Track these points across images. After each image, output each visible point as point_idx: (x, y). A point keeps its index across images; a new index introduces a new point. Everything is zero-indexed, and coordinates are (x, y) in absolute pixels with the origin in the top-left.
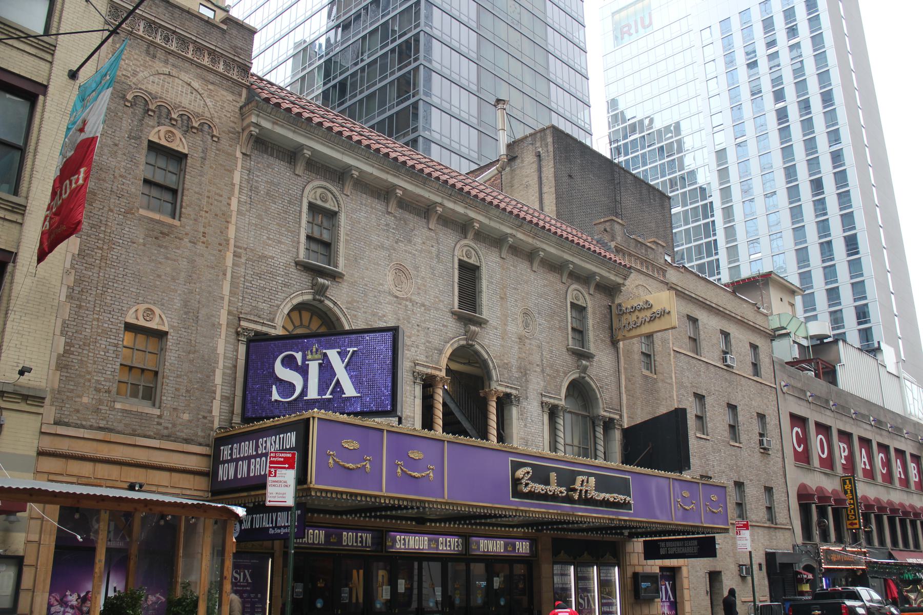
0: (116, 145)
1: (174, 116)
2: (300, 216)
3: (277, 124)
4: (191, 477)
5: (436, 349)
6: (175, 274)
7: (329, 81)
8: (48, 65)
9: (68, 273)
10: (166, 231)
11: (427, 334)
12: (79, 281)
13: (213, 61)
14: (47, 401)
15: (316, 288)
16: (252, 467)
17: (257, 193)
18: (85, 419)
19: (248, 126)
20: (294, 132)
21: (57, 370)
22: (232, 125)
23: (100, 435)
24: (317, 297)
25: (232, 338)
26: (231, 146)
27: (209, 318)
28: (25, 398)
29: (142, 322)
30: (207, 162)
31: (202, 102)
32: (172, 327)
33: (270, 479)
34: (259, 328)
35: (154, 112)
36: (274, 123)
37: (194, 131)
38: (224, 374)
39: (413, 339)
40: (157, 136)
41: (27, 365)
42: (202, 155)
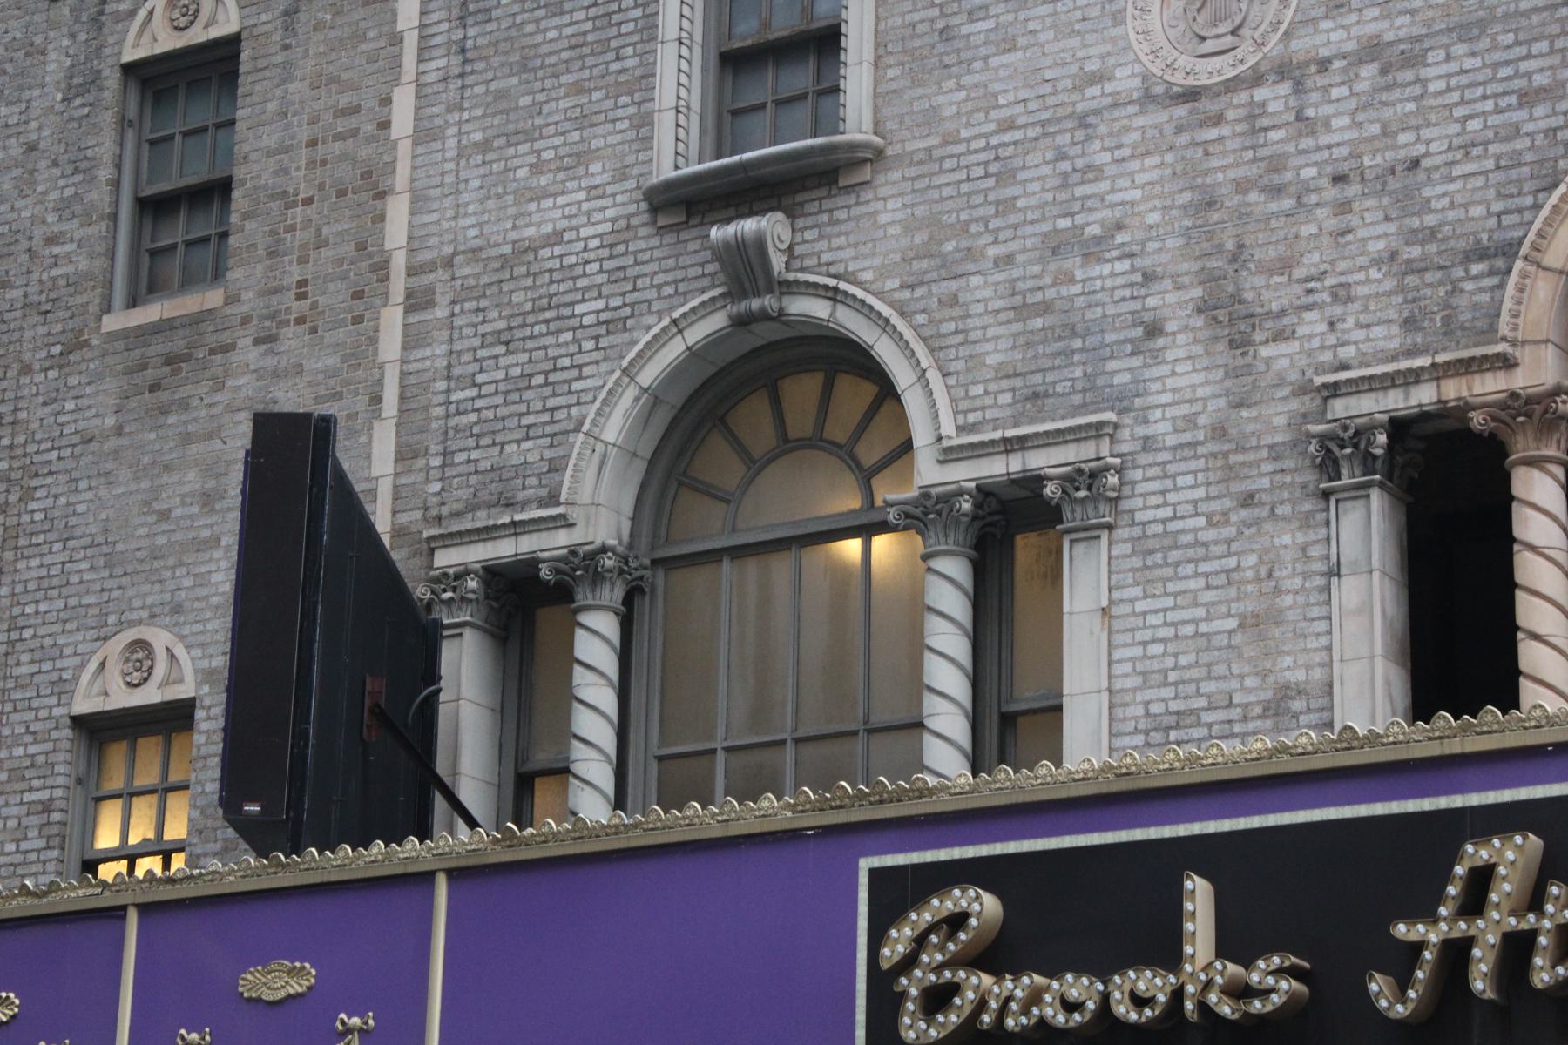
0: (32, 148)
5: (1482, 254)
6: (212, 483)
10: (179, 345)
11: (1408, 202)
24: (735, 309)
29: (123, 698)
30: (302, 16)
39: (1313, 260)
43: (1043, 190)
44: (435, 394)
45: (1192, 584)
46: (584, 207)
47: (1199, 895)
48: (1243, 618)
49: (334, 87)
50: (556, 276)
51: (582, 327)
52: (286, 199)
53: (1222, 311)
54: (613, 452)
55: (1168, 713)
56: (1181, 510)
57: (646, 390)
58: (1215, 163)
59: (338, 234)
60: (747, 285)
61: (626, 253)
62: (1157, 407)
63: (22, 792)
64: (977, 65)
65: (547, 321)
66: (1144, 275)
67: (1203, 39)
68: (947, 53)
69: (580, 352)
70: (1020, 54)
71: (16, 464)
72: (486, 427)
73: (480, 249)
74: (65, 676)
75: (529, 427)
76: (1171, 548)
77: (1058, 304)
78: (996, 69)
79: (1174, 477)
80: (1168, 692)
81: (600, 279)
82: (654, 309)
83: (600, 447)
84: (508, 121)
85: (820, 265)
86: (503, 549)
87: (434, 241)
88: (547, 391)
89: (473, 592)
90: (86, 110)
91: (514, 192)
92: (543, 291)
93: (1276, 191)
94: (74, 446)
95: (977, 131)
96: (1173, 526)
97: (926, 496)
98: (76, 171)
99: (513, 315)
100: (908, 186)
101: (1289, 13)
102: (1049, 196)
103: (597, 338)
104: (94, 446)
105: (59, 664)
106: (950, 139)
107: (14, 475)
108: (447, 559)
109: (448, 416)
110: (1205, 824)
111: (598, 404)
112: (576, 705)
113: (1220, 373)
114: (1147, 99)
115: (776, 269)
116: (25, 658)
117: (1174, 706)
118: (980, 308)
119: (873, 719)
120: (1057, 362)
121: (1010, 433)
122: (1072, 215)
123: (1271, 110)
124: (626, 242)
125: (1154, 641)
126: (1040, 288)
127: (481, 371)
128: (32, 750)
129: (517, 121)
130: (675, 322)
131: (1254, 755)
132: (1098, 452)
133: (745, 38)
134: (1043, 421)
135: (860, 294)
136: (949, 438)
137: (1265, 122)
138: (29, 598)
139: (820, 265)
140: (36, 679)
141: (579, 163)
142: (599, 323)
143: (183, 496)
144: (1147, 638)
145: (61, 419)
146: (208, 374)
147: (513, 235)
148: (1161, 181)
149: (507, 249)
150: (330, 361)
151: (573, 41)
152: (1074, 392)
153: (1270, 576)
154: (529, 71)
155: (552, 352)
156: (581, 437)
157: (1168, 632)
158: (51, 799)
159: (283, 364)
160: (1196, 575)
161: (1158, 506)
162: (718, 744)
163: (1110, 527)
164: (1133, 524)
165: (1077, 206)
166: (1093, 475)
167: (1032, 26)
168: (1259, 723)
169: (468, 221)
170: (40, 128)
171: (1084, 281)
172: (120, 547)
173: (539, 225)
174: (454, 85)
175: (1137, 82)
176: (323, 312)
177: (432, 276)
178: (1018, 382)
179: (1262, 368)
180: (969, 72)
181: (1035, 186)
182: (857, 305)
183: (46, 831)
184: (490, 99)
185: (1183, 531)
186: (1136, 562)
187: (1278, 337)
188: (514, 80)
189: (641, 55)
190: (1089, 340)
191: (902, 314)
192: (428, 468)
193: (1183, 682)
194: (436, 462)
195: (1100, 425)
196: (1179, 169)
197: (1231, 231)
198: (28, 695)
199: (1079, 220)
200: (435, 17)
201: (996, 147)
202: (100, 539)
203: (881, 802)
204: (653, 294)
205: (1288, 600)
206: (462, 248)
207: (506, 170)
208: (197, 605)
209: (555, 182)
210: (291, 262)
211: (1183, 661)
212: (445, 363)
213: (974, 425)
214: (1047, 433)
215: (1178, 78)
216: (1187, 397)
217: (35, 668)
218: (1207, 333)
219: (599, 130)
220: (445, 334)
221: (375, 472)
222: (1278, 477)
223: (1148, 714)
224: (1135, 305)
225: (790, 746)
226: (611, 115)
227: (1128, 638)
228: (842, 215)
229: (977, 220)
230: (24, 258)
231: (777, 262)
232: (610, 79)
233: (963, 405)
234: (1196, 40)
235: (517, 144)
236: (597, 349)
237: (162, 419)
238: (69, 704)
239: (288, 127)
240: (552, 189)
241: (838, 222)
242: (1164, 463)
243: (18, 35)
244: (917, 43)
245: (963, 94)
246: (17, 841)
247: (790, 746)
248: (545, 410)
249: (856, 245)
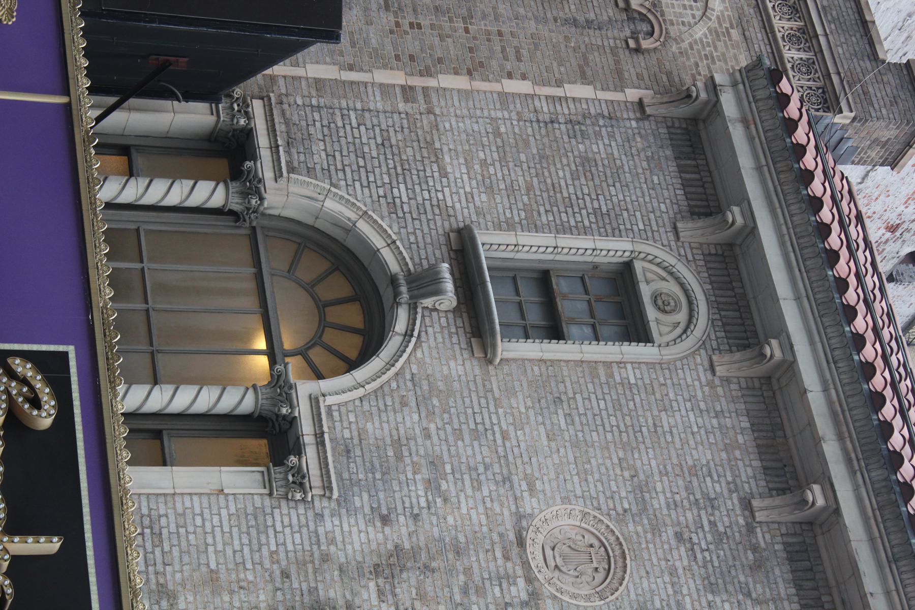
3: (747, 127)
20: (759, 168)
24: (401, 277)
26: (639, 77)
30: (573, 29)
36: (744, 121)
42: (581, 19)
43: (467, 457)
44: (354, 102)
45: (236, 543)
46: (462, 190)
47: (49, 545)
48: (217, 572)
49: (532, 47)
50: (421, 173)
51: (392, 188)
52: (468, 18)
53: (396, 560)
54: (318, 205)
55: (161, 528)
56: (280, 536)
57: (354, 224)
58: (481, 556)
59: (448, 47)
60: (414, 285)
61: (434, 214)
62: (341, 522)
64: (540, 419)
65: (395, 168)
66: (417, 515)
67: (553, 549)
68: (547, 401)
69: (377, 187)
70: (546, 443)
72: (334, 131)
73: (438, 130)
75: (334, 156)
76: (258, 530)
77: (401, 465)
78: (537, 430)
79: (300, 532)
80: (173, 528)
81: (420, 199)
82: (402, 230)
83: (321, 197)
84: (511, 147)
85: (426, 326)
86: (262, 140)
87: (443, 103)
88: (355, 167)
89: (238, 122)
91: (470, 150)
92: (413, 166)
93: (465, 592)
95: (502, 418)
96: (271, 532)
97: (291, 387)
99: (399, 148)
100: (471, 378)
101: (566, 598)
102: (464, 460)
103: (385, 197)
106: (497, 403)
108: (257, 107)
109: (341, 109)
110: (92, 549)
111: (347, 196)
112: (170, 181)
113: (360, 559)
114: (519, 517)
115: (423, 301)
117: (165, 531)
118: (400, 419)
119: (160, 355)
120: (368, 464)
121: (326, 436)
122: (453, 473)
123: (512, 588)
124: (441, 214)
125: (203, 520)
126: (411, 454)
127: (367, 129)
129: (511, 152)
130: (394, 242)
131: (132, 578)
132: (315, 487)
133: (557, 285)
134: (333, 455)
135: (409, 350)
136: (324, 401)
137: (505, 585)
139: (426, 326)
141: (486, 188)
142: (394, 198)
144: (205, 515)
147: (445, 149)
148: (472, 525)
149: (437, 145)
150: (373, 41)
151: (557, 185)
152: (350, 474)
153: (241, 588)
154: (540, 160)
155: (377, 170)
156: (327, 186)
157: (208, 528)
159: (373, 14)
160: (242, 545)
161: (282, 522)
162: (146, 264)
163: (270, 494)
164: (273, 508)
165: (458, 476)
166: (301, 485)
167: (562, 450)
168: (154, 581)
169: (454, 123)
171: (414, 480)
173: (451, 164)
174: (532, 116)
175: (529, 511)
176: (402, 38)
177: (423, 102)
178: (356, 441)
179: (362, 584)
180: (536, 414)
181: (470, 452)
182: (402, 348)
184: (524, 136)
185: (268, 537)
186: (250, 510)
187: (380, 593)
188: (535, 151)
189: (548, 225)
190: (380, 483)
191: (397, 374)
192: (311, 97)
193: (179, 537)
194: (314, 102)
195: (331, 489)
196: (479, 535)
197: (442, 565)
199: (450, 477)
200: (572, 106)
201: (492, 429)
203: (107, 359)
204: (410, 230)
205: (227, 598)
206: (438, 119)
207: (483, 146)
209: (476, 173)
210: (431, 20)
211: (191, 537)
212: (372, 108)
213: (332, 416)
214: (326, 458)
215: (531, 535)
216: (346, 540)
218: (383, 551)
219: (506, 200)
220: (389, 108)
221: (308, 66)
222: (298, 592)
223: (160, 516)
224: (400, 509)
225: (144, 306)
226: (514, 207)
227: (206, 505)
228: (455, 339)
229: (450, 418)
231: (428, 302)
232: (535, 207)
233: (343, 409)
234: (552, 545)
235: (498, 152)
236: (379, 197)
239: (510, 19)
240: (472, 172)
241: (451, 337)
242: (308, 526)
244: (553, 384)
245: (523, 410)
247: (144, 306)
248: (344, 166)
249: (437, 348)
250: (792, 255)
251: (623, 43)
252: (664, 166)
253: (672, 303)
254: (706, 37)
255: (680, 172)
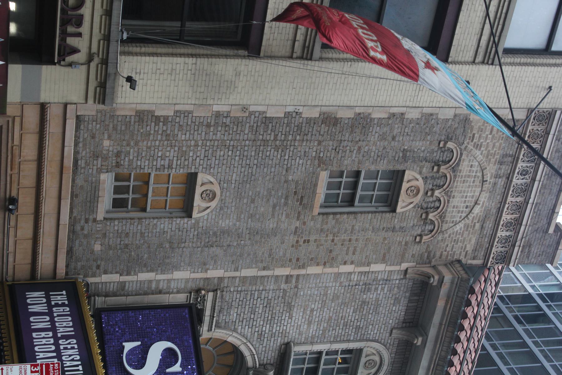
0: (394, 138)
1: (437, 193)
2: (344, 341)
4: (29, 260)
6: (257, 217)
7: (544, 301)
8: (471, 59)
9: (244, 109)
10: (305, 201)
12: (237, 122)
13: (508, 225)
14: (101, 107)
15: (261, 370)
16: (43, 334)
17: (363, 292)
18: (85, 145)
19: (439, 273)
20: (441, 324)
21: (136, 112)
22: (438, 254)
23: (69, 162)
25: (191, 285)
26: (413, 256)
27: (212, 258)
28: (103, 85)
29: (199, 190)
31: (458, 219)
32: (198, 221)
33: (28, 366)
34: (208, 313)
35: (438, 171)
37: (424, 216)
38: (150, 282)
40: (411, 178)
41: (138, 87)
42: (397, 227)
61: (278, 337)
63: (177, 157)
65: (268, 317)
71: (289, 143)
73: (296, 296)
74: (212, 169)
81: (274, 331)
88: (248, 319)
90: (396, 159)
91: (308, 305)
92: (277, 315)
94: (287, 165)
98: (378, 156)
103: (258, 332)
104: (284, 172)
105: (216, 166)
107: (285, 142)
116: (222, 153)
128: (191, 159)
138: (242, 153)
140: (214, 158)
143: (257, 207)
145: (298, 158)
146: (293, 212)
147: (296, 305)
149: (293, 304)
151: (344, 317)
155: (259, 320)
158: (172, 168)
169: (306, 291)
170: (399, 141)
172: (248, 186)
173: (296, 312)
183: (162, 167)
188: (340, 301)
198: (209, 156)
202: (253, 179)
204: (264, 345)
206: (299, 290)
208: (221, 215)
217: (218, 158)
220: (275, 288)
230: (357, 140)
232: (328, 328)
237: (284, 197)
238: (202, 172)
243: (434, 129)
246: (161, 157)
248: (243, 319)
250: (432, 365)
251: (414, 238)
252: (402, 301)
253: (373, 364)
254: (461, 230)
255: (408, 303)
